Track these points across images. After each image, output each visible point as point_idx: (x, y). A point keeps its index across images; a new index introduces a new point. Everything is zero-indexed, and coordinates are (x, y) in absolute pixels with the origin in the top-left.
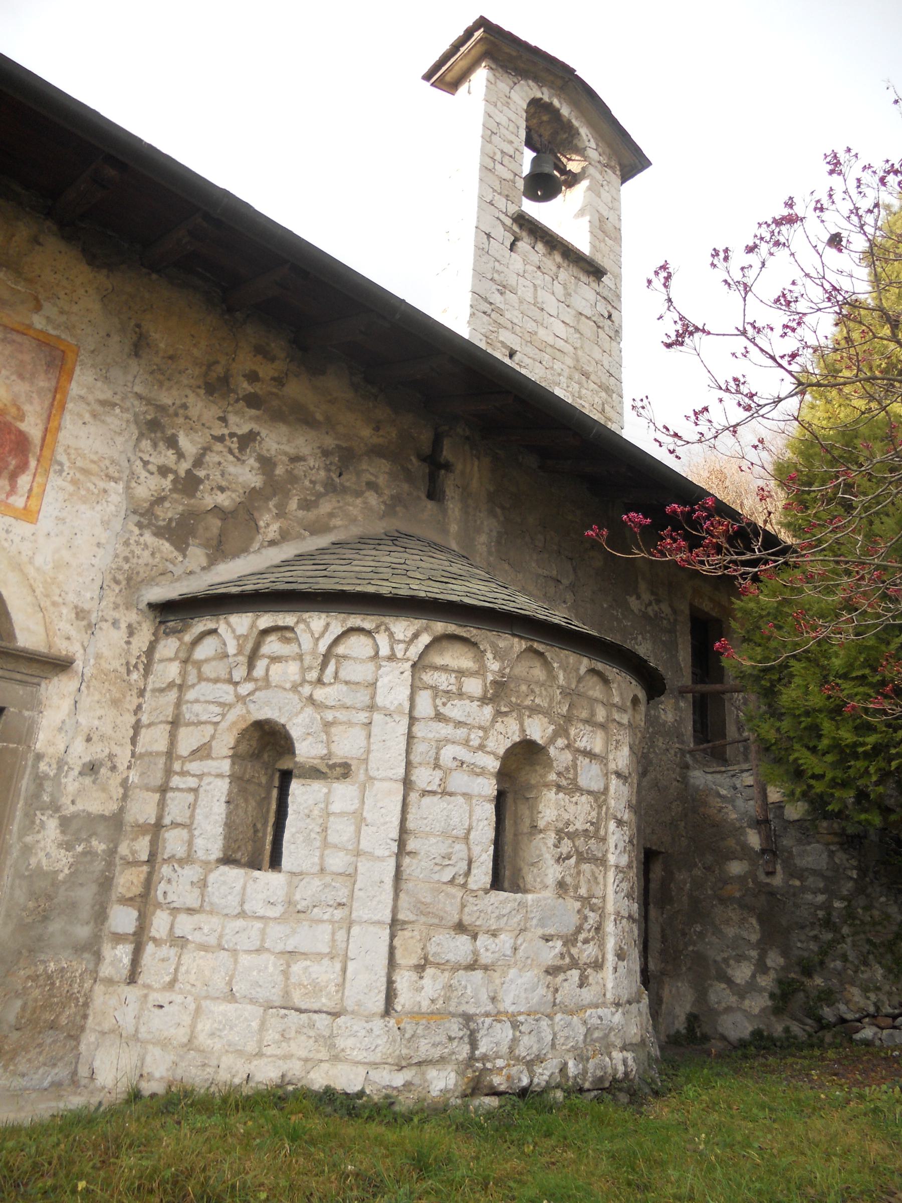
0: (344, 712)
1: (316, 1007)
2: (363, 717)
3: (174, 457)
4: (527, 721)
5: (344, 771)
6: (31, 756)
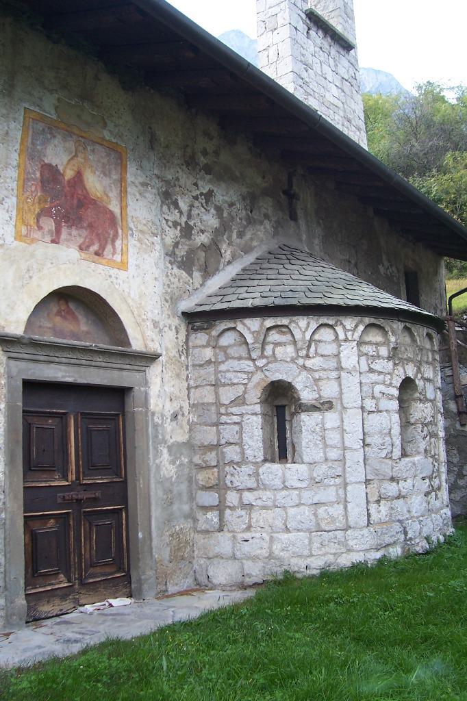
0: (324, 372)
1: (334, 528)
2: (334, 374)
3: (178, 214)
4: (406, 367)
5: (329, 405)
6: (149, 414)
